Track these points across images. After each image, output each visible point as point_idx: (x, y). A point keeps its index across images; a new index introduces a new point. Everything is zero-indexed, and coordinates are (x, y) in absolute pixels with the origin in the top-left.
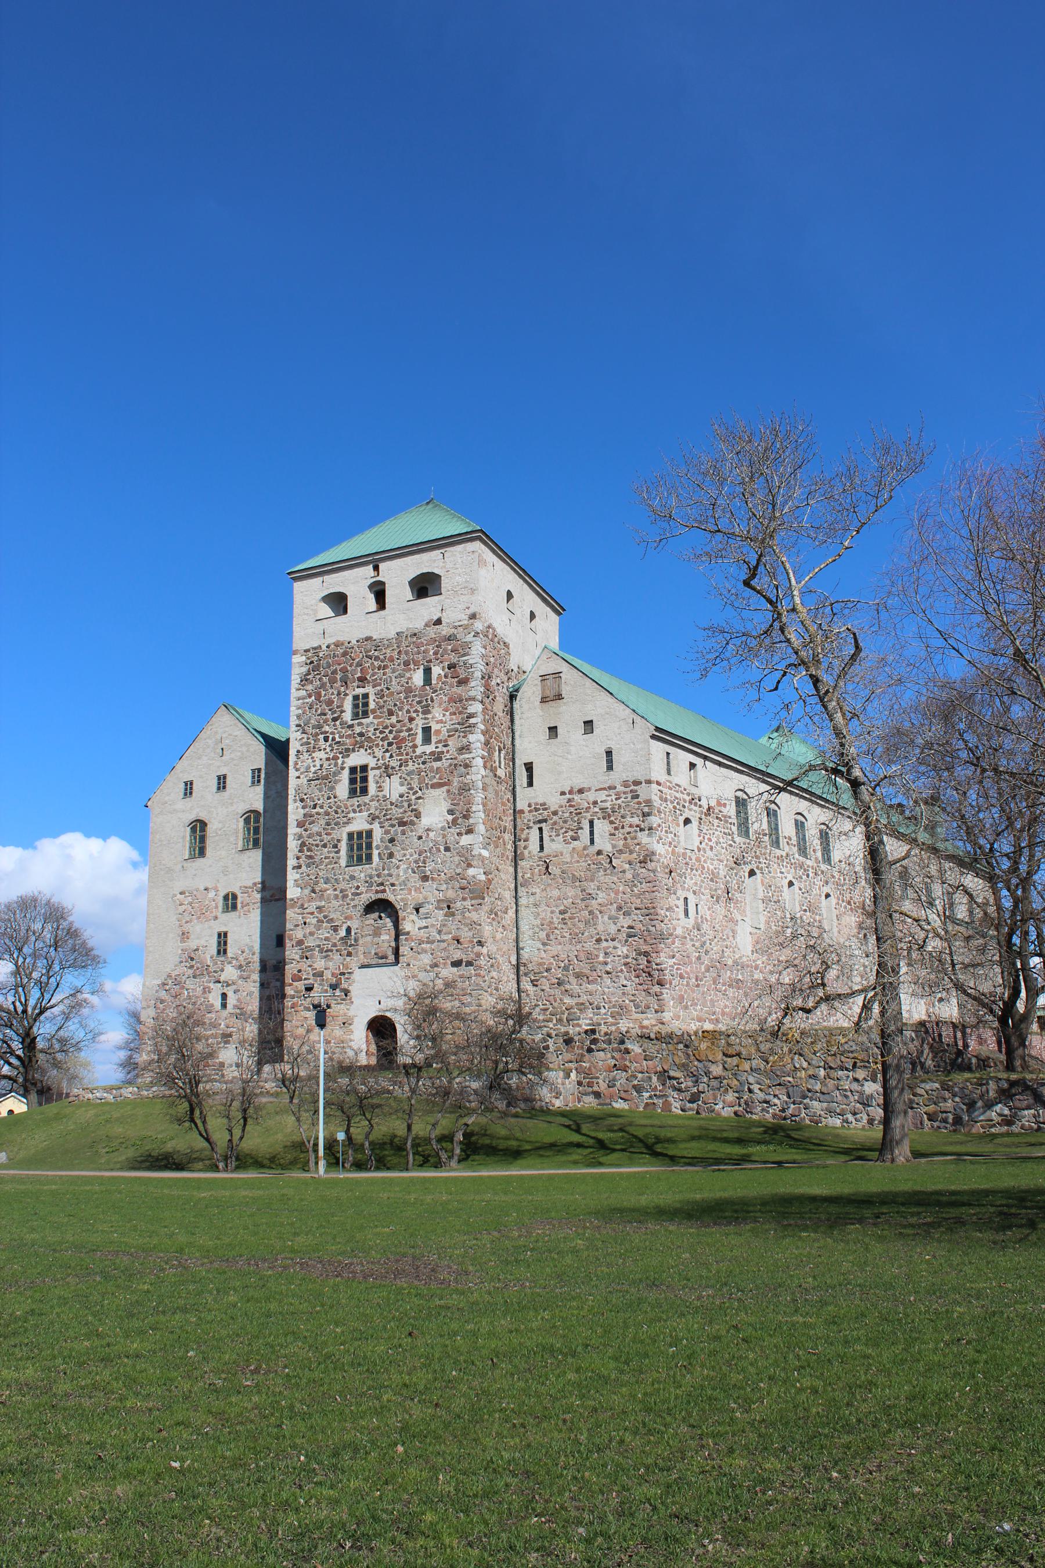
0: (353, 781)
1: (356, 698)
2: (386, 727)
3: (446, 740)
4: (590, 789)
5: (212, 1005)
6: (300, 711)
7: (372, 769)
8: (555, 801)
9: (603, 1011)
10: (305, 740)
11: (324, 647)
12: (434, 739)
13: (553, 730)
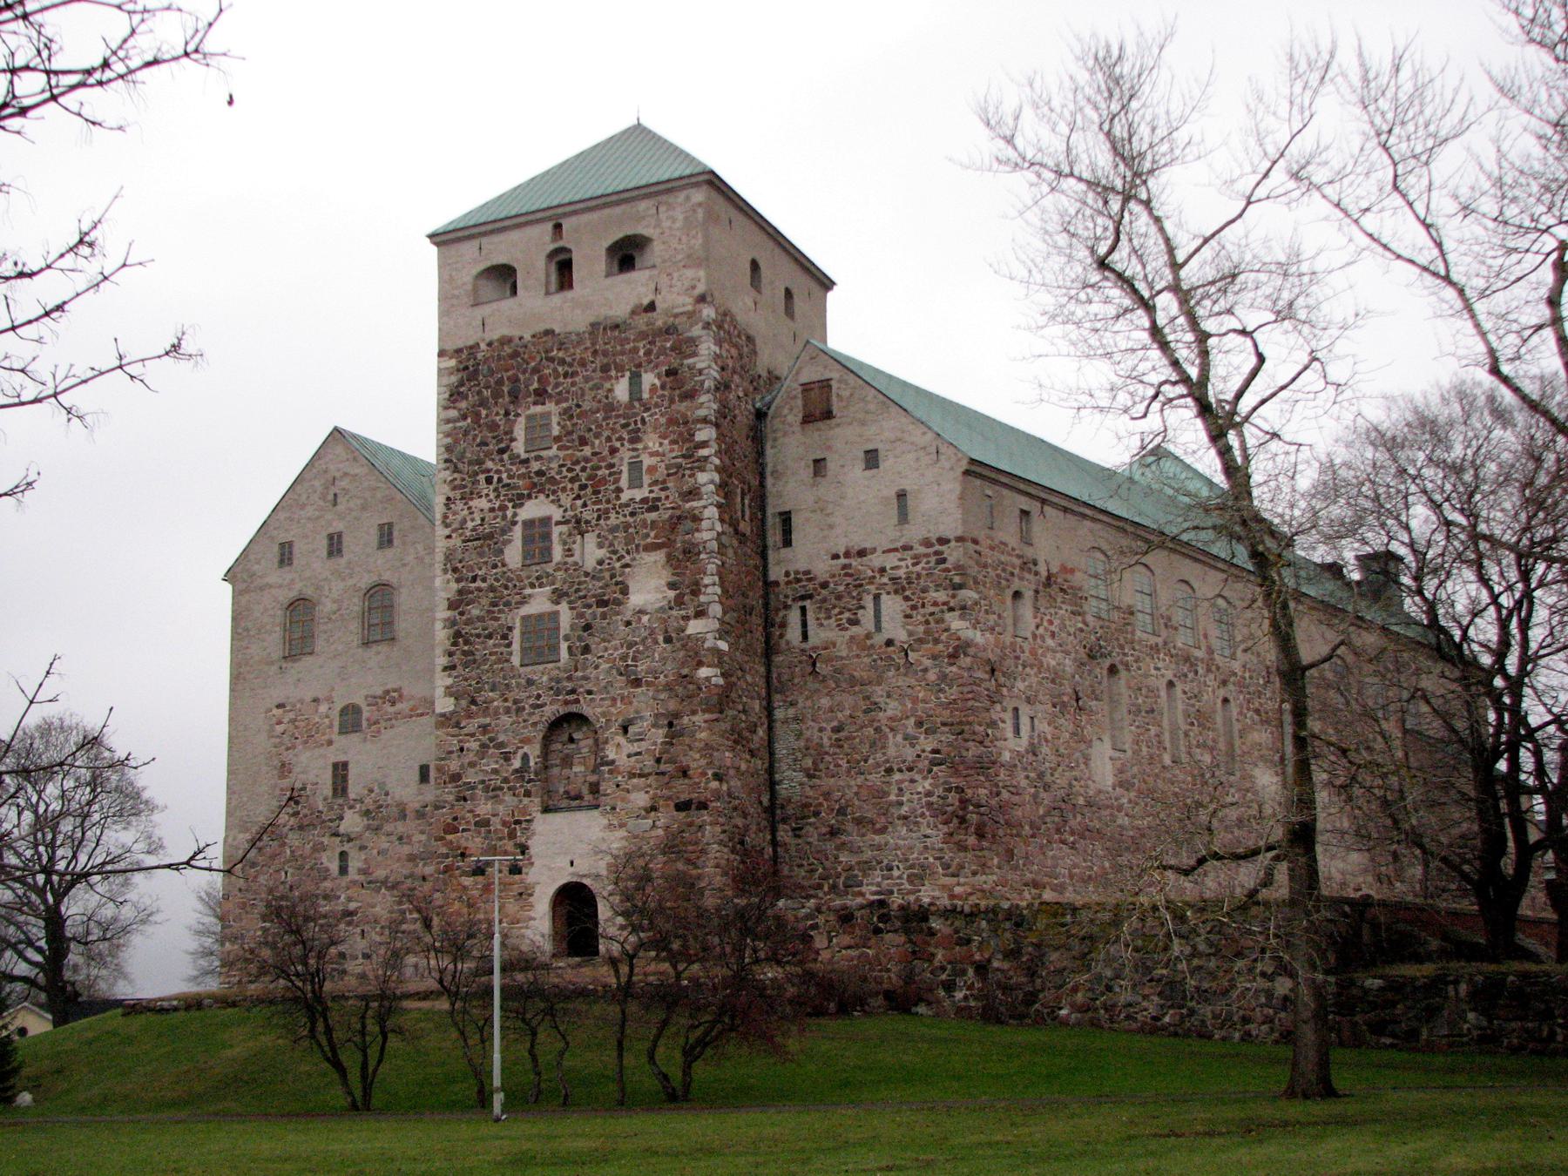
0: (527, 540)
3: (664, 482)
4: (874, 550)
5: (327, 870)
6: (449, 440)
7: (558, 523)
8: (822, 568)
9: (896, 873)
10: (457, 482)
11: (483, 346)
12: (646, 479)
13: (819, 465)
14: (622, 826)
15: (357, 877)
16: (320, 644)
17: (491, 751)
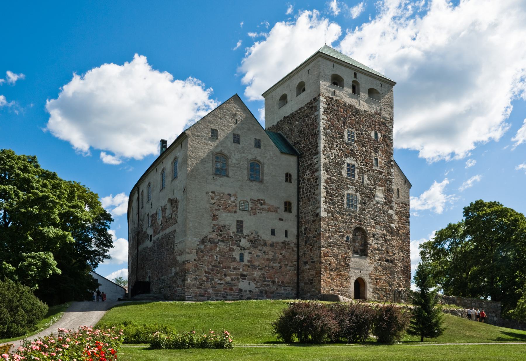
0: (348, 170)
5: (235, 258)
14: (373, 263)
15: (247, 263)
16: (231, 173)
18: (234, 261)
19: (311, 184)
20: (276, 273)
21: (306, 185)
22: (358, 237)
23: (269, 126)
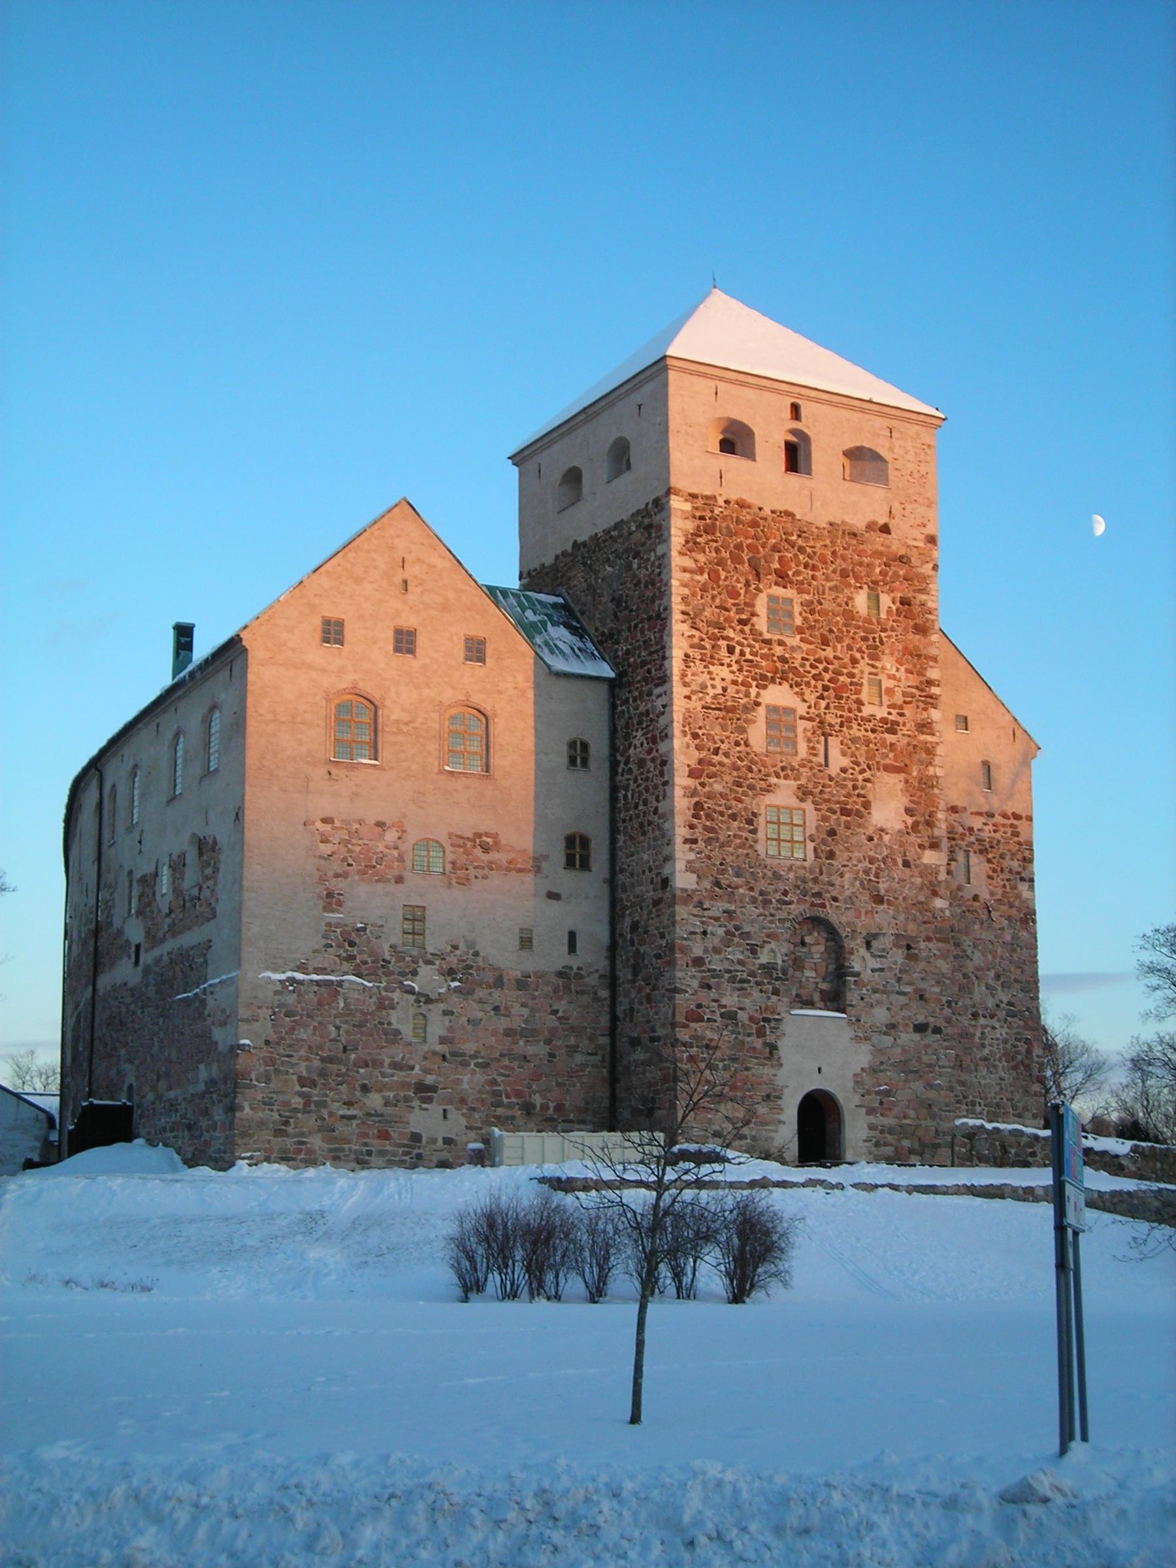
1: (772, 598)
2: (819, 661)
3: (901, 707)
5: (397, 1033)
6: (686, 591)
7: (801, 718)
10: (696, 640)
11: (721, 502)
14: (867, 1039)
15: (438, 1048)
17: (736, 940)
18: (394, 1042)
19: (647, 779)
20: (536, 1077)
21: (636, 781)
22: (814, 949)
23: (532, 567)
